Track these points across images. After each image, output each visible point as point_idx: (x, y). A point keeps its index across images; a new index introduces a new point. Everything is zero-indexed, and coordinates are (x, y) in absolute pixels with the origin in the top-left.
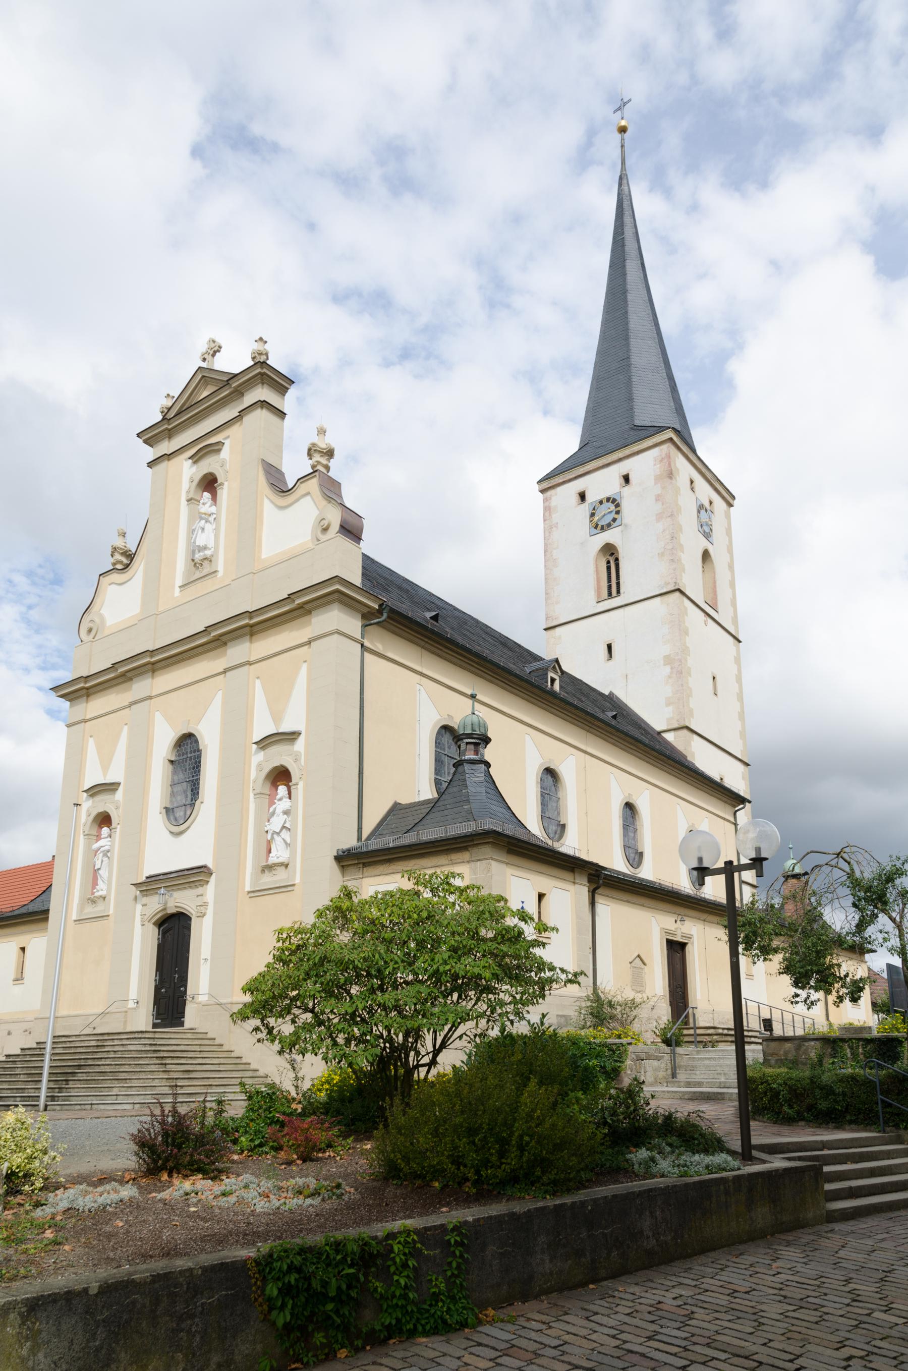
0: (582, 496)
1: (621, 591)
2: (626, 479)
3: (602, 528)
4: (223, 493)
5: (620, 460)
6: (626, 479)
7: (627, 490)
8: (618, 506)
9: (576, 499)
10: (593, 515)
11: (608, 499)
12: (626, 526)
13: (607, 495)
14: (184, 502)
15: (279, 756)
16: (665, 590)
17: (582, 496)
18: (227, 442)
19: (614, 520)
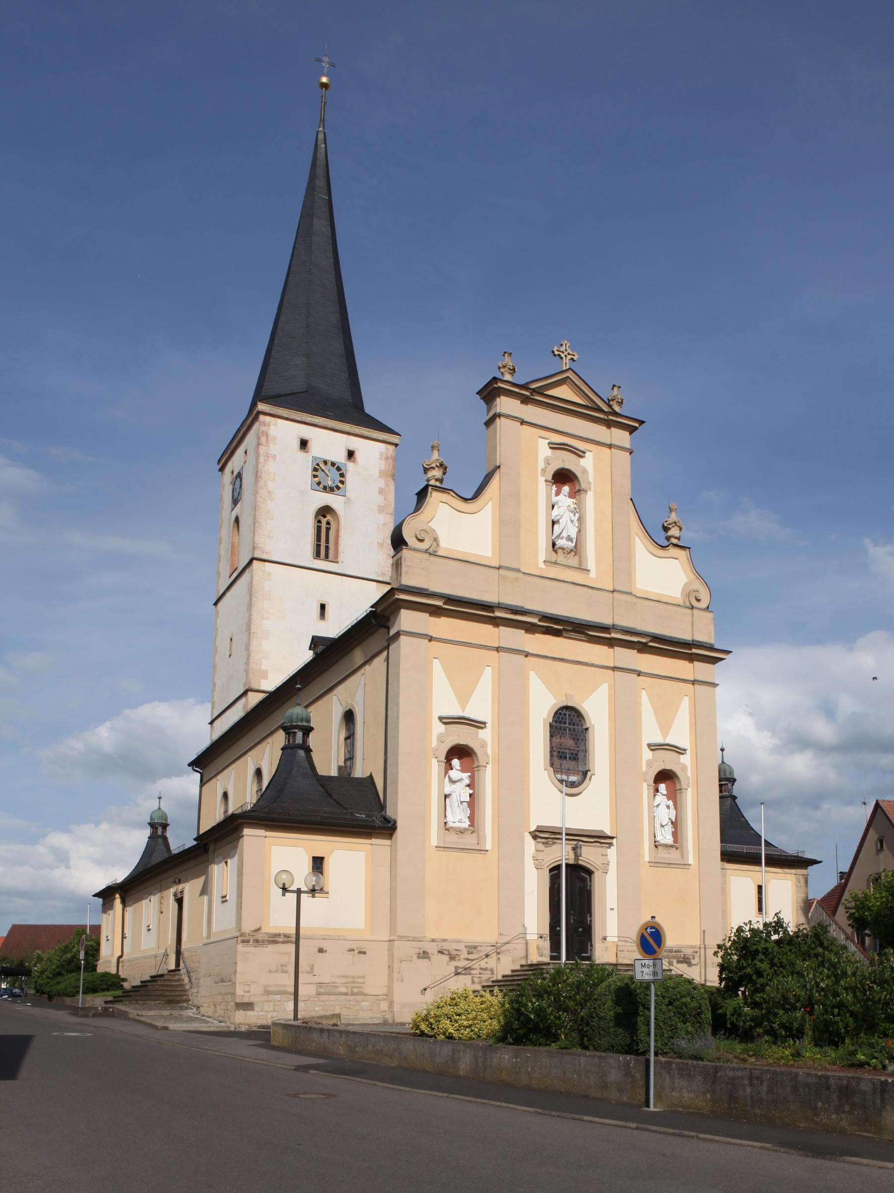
0: (304, 444)
1: (340, 559)
2: (351, 454)
3: (325, 488)
4: (589, 499)
5: (349, 434)
6: (351, 454)
7: (350, 466)
8: (342, 475)
9: (297, 444)
10: (315, 470)
11: (333, 464)
12: (349, 499)
13: (334, 460)
14: (541, 481)
15: (667, 761)
16: (380, 579)
17: (304, 444)
18: (588, 454)
19: (338, 488)
